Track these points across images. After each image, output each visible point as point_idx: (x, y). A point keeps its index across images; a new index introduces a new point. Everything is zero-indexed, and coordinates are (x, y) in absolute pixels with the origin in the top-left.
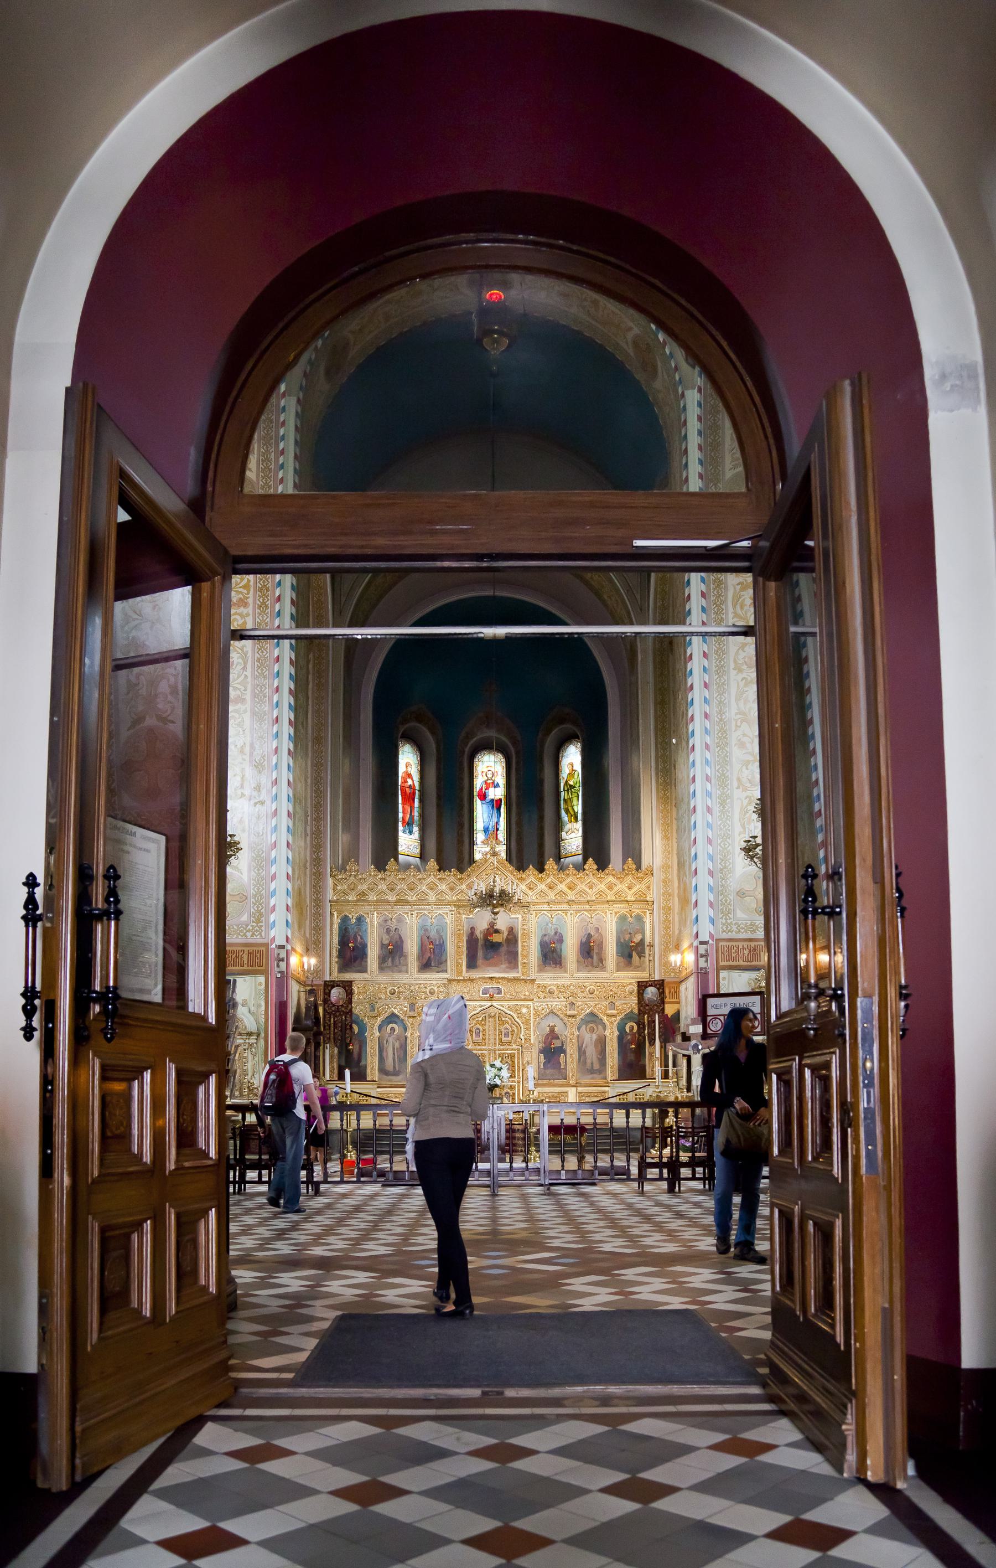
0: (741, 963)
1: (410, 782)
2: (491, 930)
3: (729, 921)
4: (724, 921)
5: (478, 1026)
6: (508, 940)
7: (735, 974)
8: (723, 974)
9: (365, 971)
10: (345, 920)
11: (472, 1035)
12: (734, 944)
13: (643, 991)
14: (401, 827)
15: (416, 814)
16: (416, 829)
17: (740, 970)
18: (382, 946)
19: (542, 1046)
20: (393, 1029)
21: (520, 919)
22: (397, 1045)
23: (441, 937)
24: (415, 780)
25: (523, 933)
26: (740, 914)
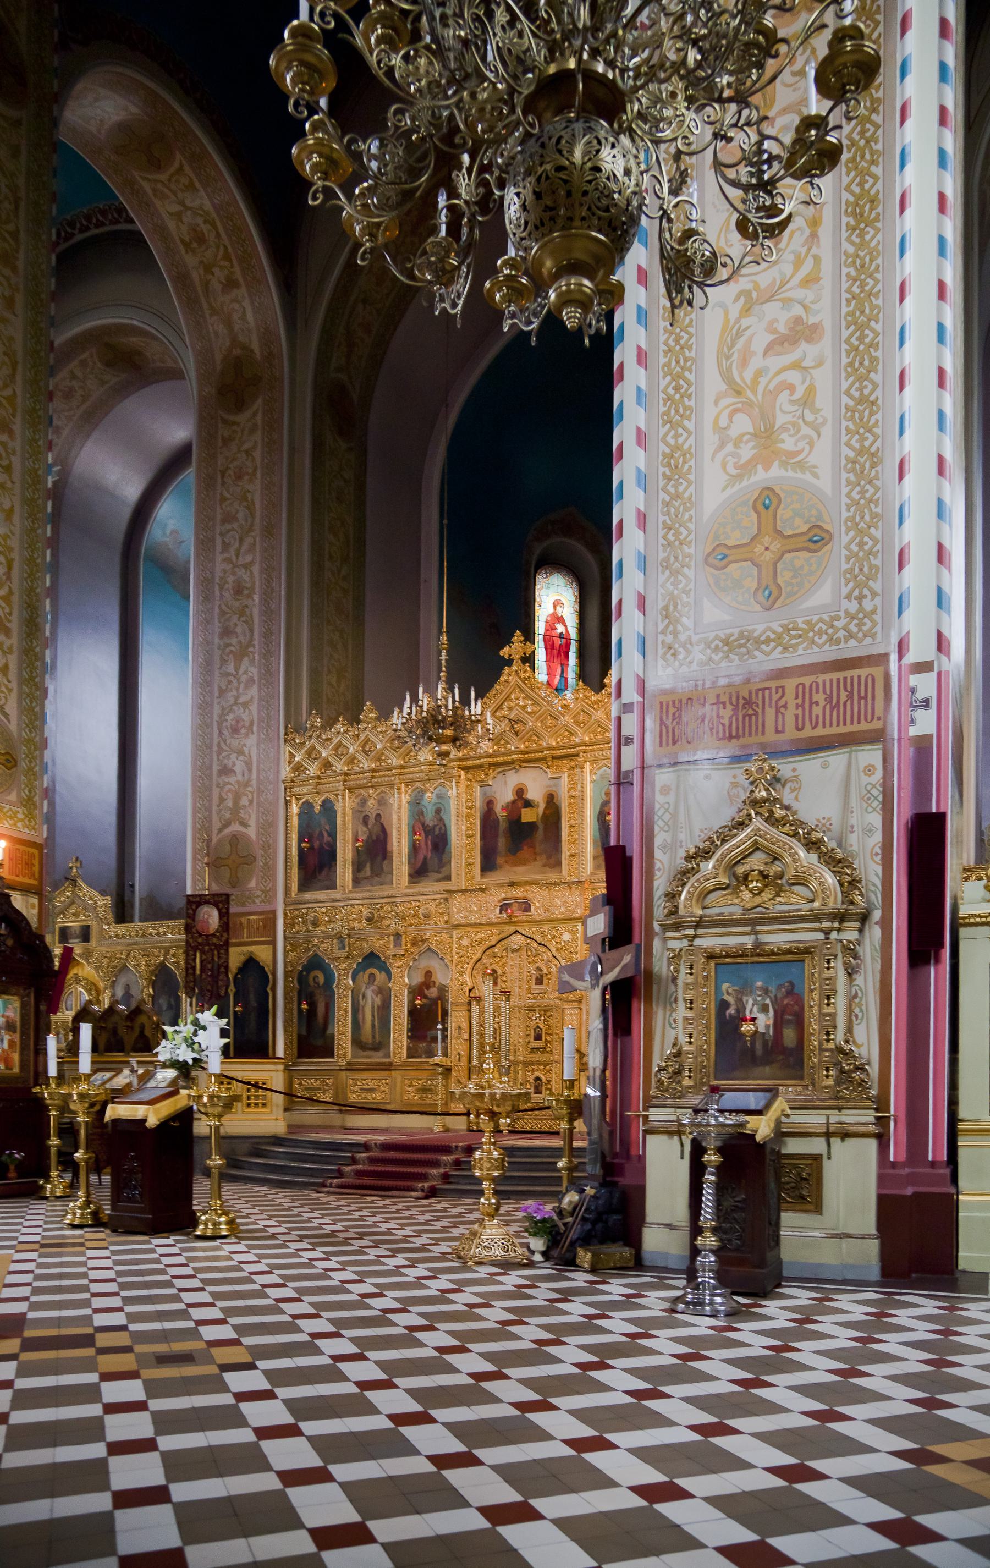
9: (333, 886)
10: (307, 808)
23: (441, 820)
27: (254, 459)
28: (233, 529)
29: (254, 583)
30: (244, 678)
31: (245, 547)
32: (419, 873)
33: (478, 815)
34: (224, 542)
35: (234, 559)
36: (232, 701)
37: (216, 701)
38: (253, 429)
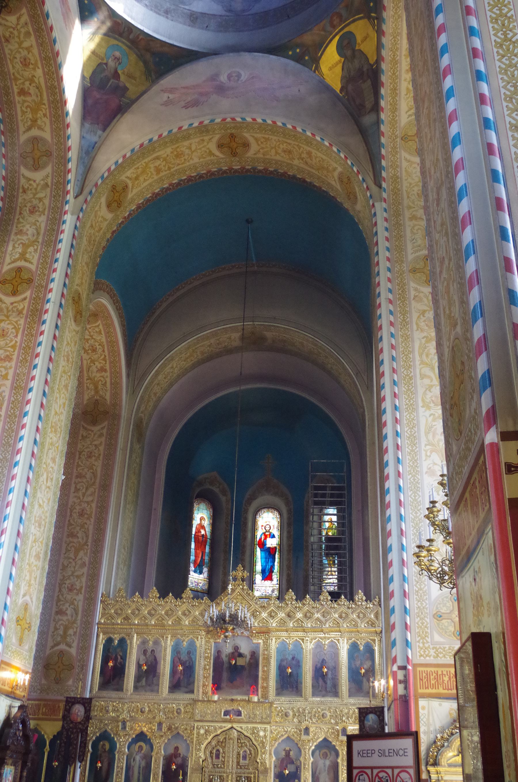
0: (441, 691)
1: (203, 532)
2: (237, 653)
3: (426, 645)
4: (421, 645)
5: (218, 747)
6: (250, 664)
7: (435, 703)
8: (422, 703)
10: (109, 641)
11: (212, 757)
12: (433, 669)
13: (364, 717)
14: (192, 568)
15: (207, 558)
16: (205, 570)
17: (440, 698)
18: (139, 666)
19: (278, 770)
20: (141, 748)
21: (262, 644)
22: (143, 764)
23: (191, 658)
24: (207, 531)
25: (264, 658)
26: (437, 638)
27: (99, 450)
28: (82, 482)
29: (92, 512)
30: (79, 562)
31: (89, 492)
32: (175, 687)
33: (212, 658)
34: (76, 487)
35: (81, 498)
36: (70, 573)
37: (60, 571)
38: (101, 435)
